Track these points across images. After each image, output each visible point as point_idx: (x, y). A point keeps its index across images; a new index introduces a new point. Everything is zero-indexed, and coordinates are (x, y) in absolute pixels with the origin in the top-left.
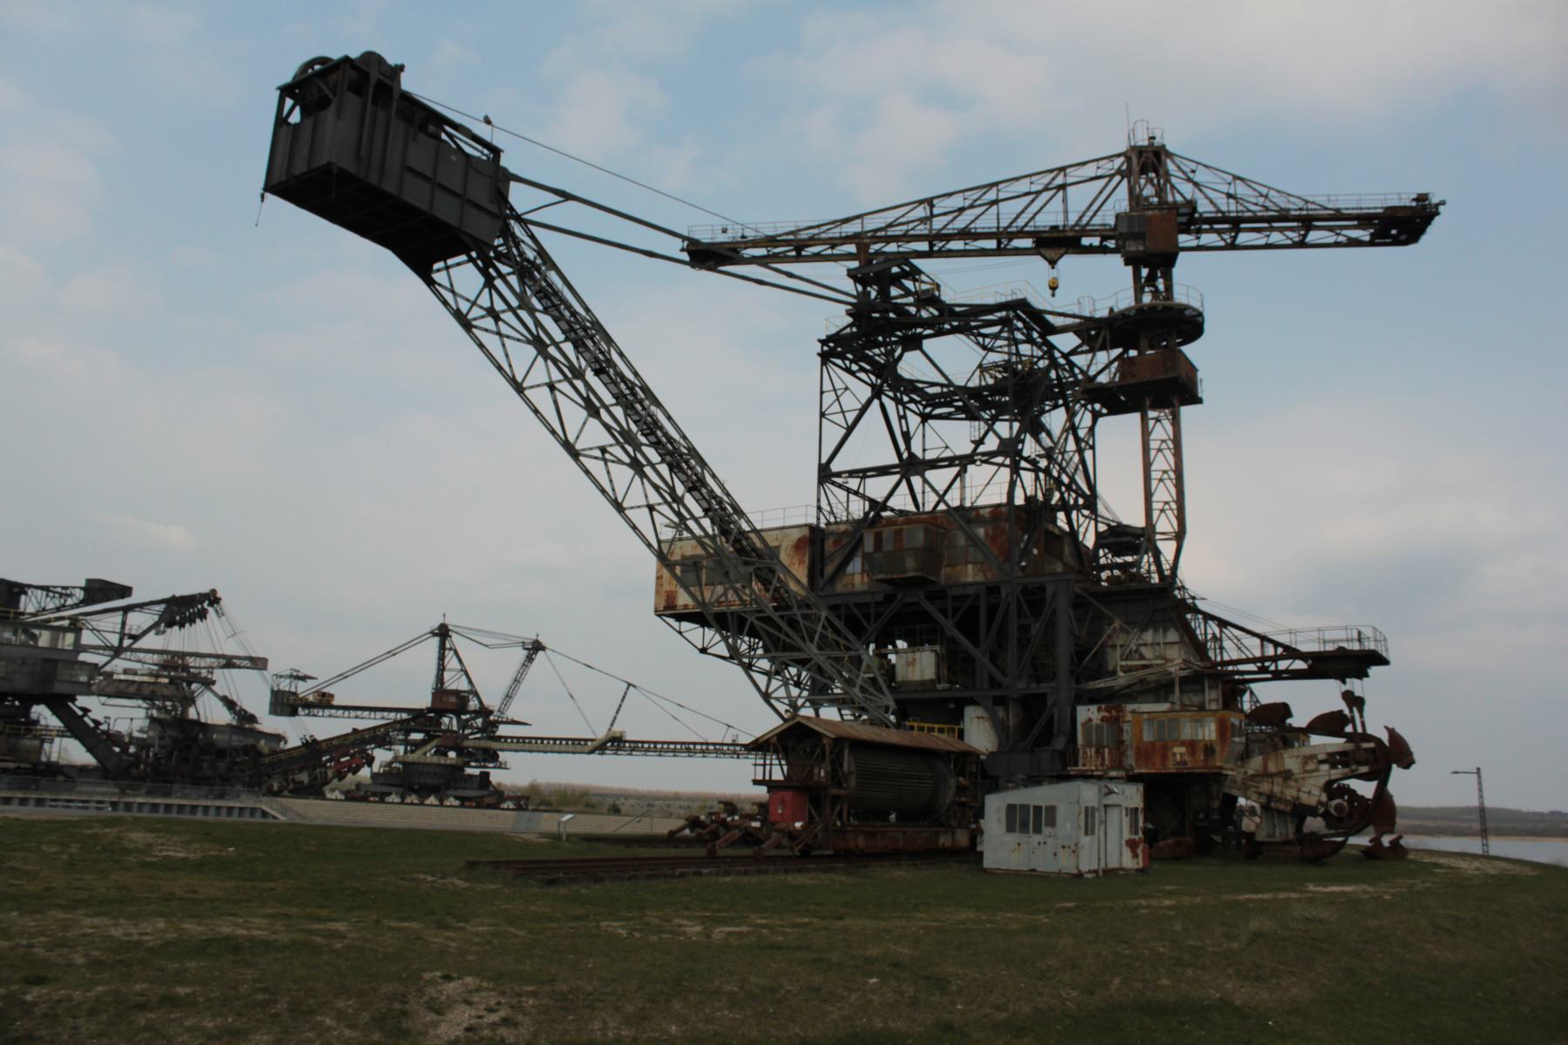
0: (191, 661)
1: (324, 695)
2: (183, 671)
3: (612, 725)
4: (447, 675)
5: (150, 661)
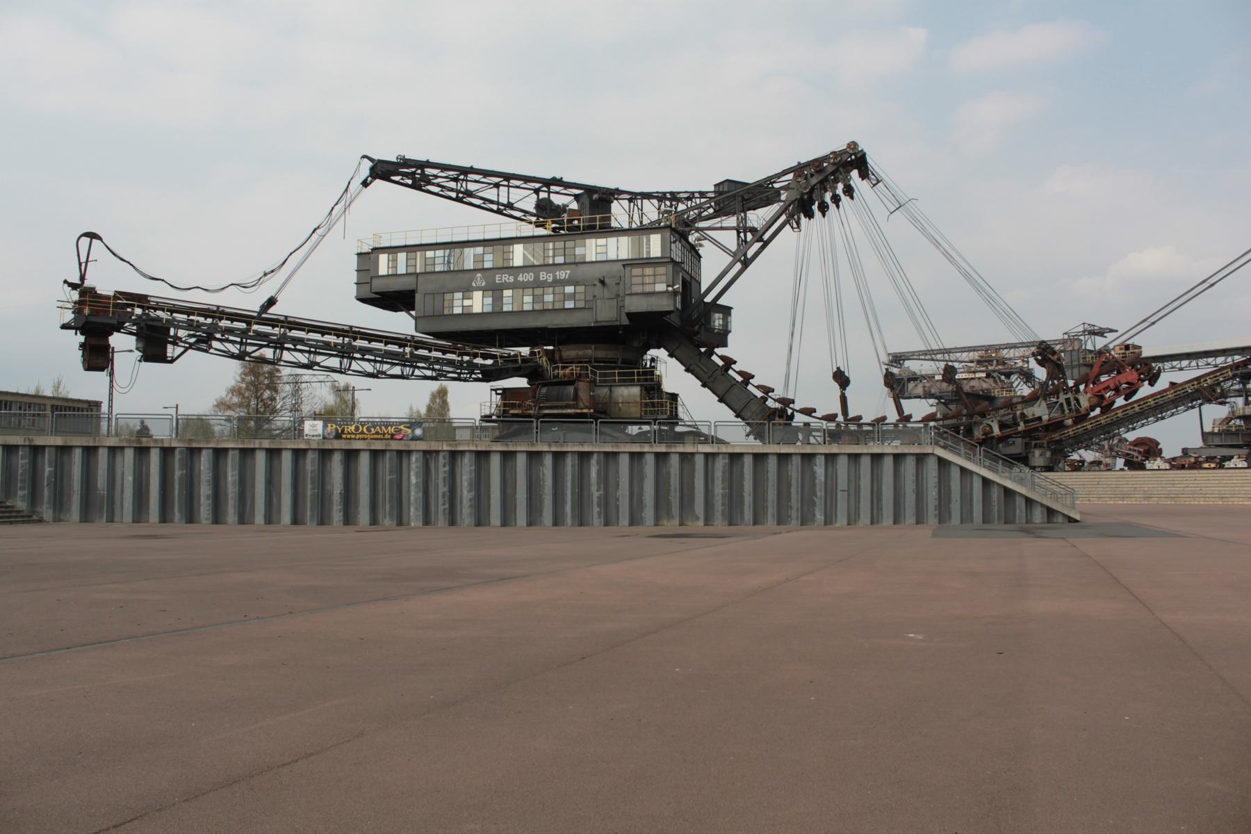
0: (1005, 353)
1: (1127, 347)
2: (998, 364)
5: (967, 360)
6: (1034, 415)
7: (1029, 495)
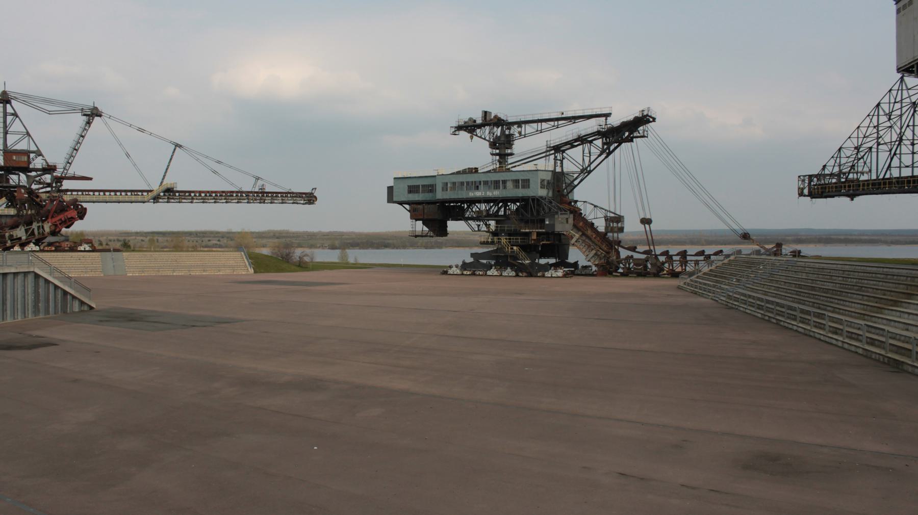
3: (163, 179)
4: (11, 139)
6: (17, 236)
7: (75, 295)
